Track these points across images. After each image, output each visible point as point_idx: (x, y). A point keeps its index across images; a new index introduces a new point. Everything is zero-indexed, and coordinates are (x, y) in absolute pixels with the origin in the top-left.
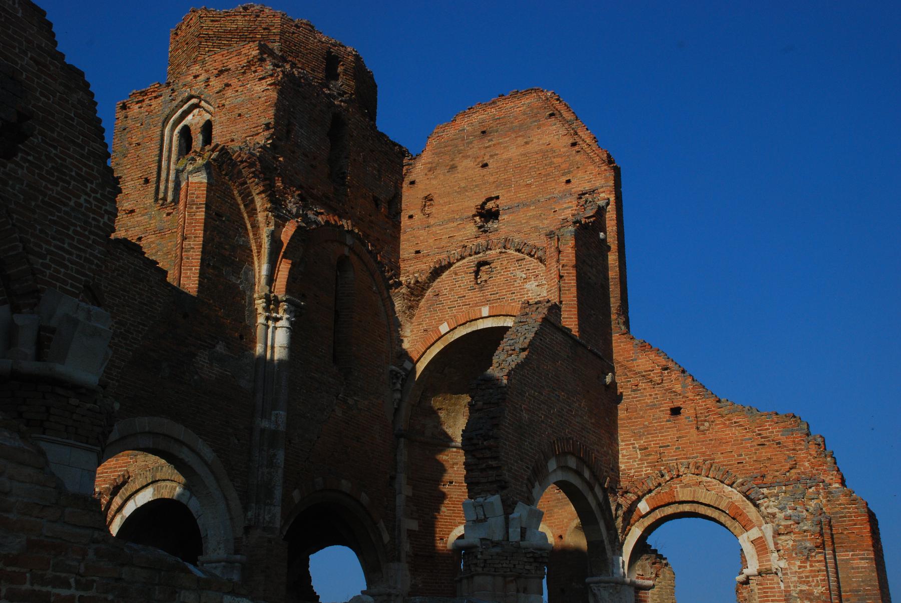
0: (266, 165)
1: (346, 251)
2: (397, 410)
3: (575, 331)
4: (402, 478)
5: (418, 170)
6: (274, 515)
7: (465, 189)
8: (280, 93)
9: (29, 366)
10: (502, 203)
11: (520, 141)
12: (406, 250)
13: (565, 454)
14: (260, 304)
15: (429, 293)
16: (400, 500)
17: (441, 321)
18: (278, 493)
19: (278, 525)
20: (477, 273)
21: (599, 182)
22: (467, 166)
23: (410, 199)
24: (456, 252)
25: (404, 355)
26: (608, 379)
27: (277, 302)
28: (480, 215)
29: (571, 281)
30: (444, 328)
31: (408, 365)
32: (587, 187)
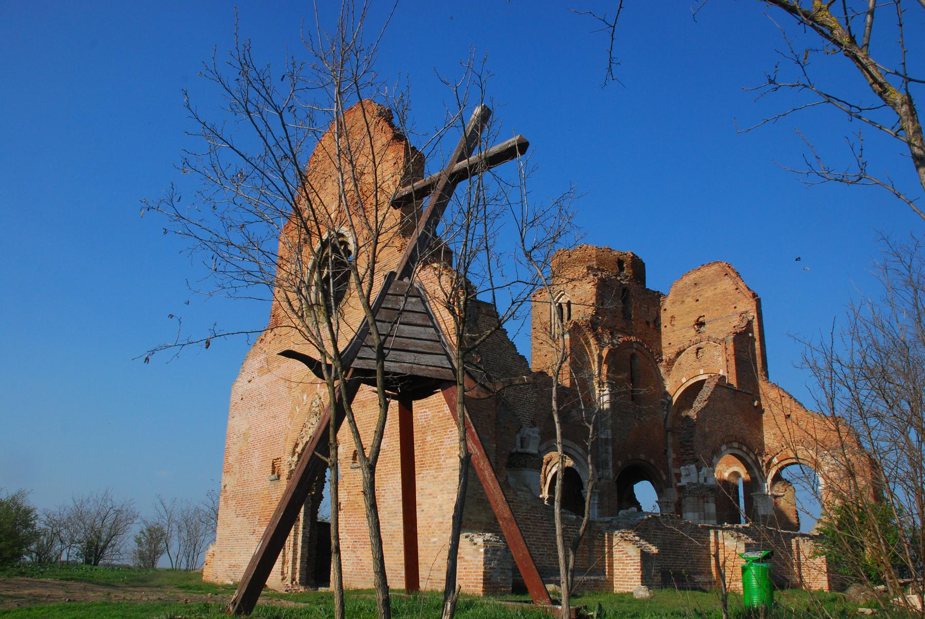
0: (593, 325)
1: (634, 351)
2: (665, 420)
3: (735, 385)
4: (670, 450)
5: (667, 304)
6: (610, 473)
7: (689, 312)
8: (597, 288)
9: (520, 450)
10: (706, 319)
11: (712, 288)
12: (664, 343)
13: (731, 442)
14: (596, 386)
15: (676, 363)
16: (670, 460)
17: (682, 377)
18: (611, 464)
19: (611, 477)
20: (697, 353)
21: (749, 308)
22: (689, 301)
23: (665, 318)
24: (687, 344)
25: (667, 393)
26: (756, 403)
27: (603, 383)
28: (697, 324)
29: (732, 362)
30: (684, 380)
31: (669, 398)
32: (744, 310)
